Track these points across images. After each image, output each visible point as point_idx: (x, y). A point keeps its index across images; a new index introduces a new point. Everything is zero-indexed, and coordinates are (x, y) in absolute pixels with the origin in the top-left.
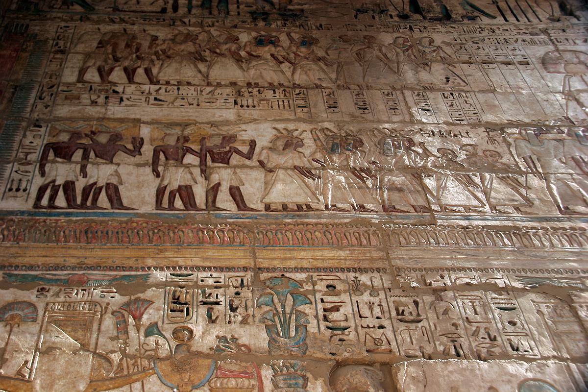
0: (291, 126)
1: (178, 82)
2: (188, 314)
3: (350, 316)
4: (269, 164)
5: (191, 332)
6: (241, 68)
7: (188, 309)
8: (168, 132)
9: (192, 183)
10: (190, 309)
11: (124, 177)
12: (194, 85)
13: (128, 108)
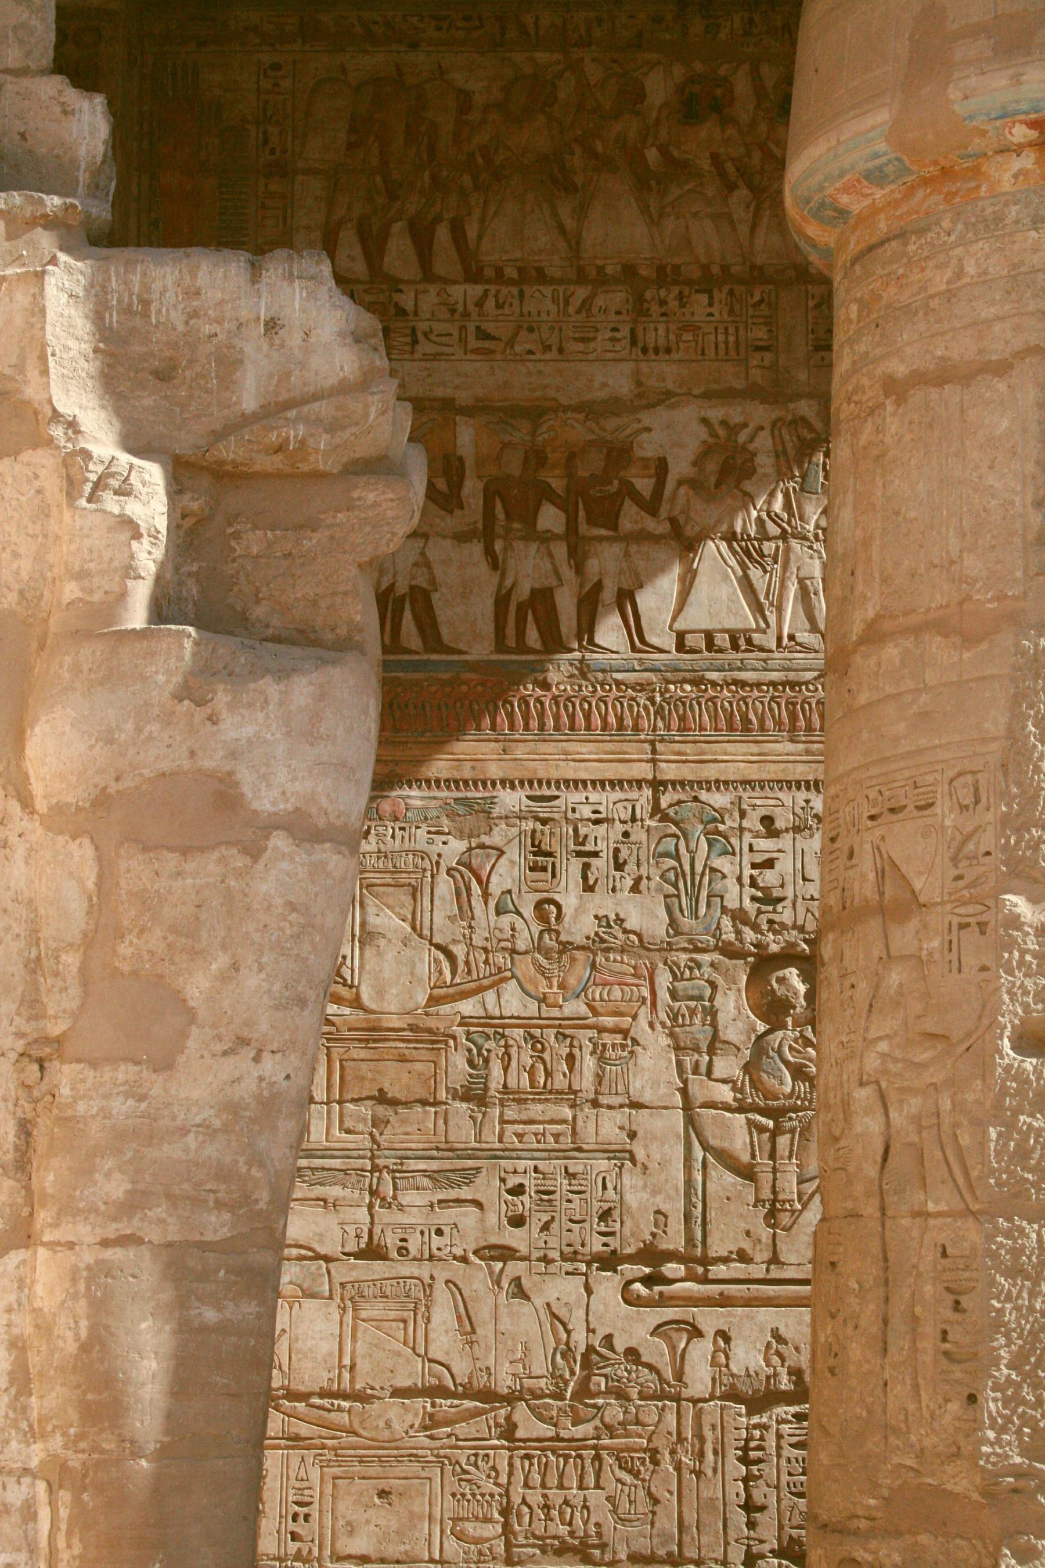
0: (735, 414)
1: (520, 270)
2: (554, 876)
3: (789, 879)
4: (688, 528)
5: (559, 907)
6: (645, 210)
7: (553, 864)
8: (507, 438)
9: (555, 583)
10: (558, 866)
11: (438, 570)
12: (552, 281)
13: (429, 364)
